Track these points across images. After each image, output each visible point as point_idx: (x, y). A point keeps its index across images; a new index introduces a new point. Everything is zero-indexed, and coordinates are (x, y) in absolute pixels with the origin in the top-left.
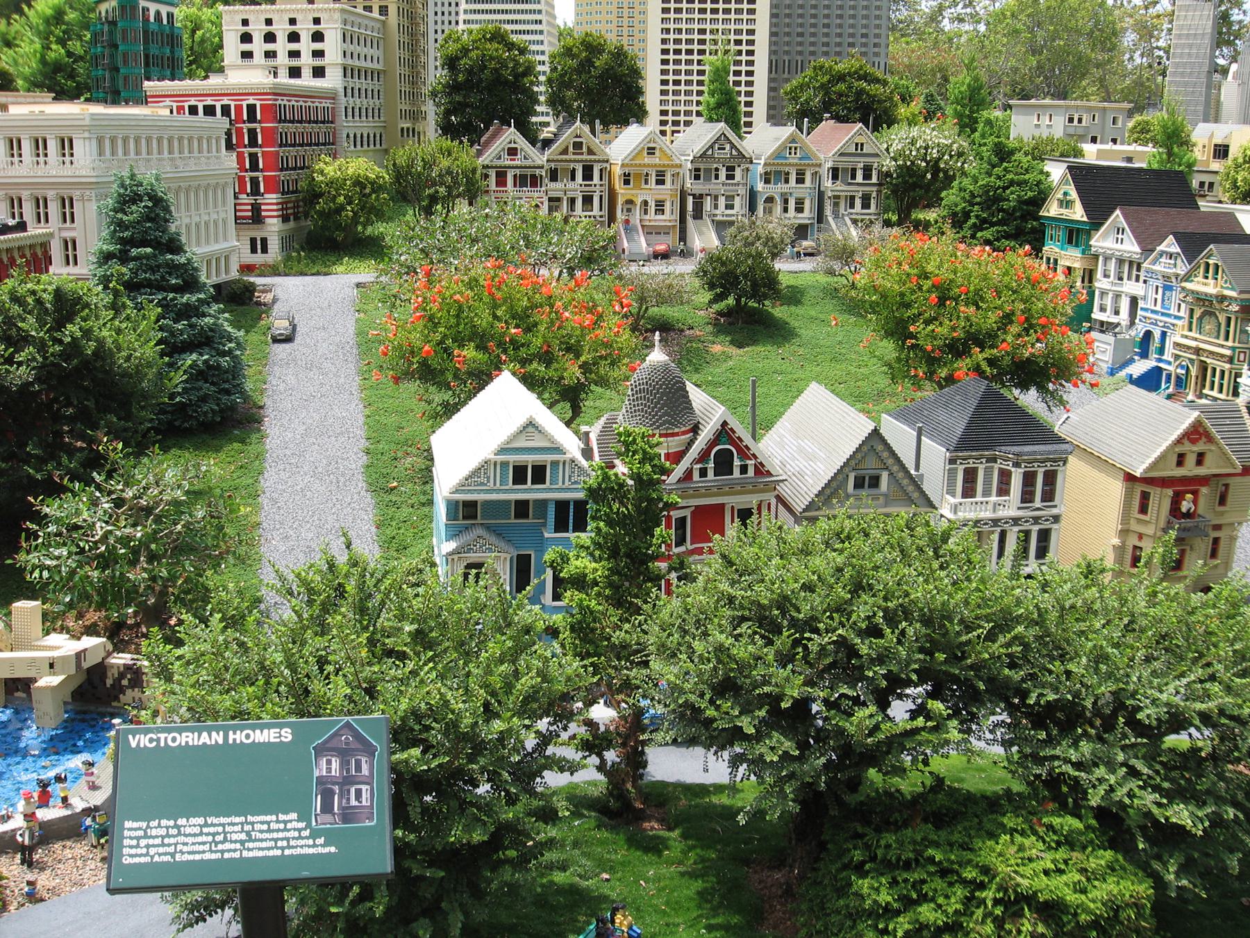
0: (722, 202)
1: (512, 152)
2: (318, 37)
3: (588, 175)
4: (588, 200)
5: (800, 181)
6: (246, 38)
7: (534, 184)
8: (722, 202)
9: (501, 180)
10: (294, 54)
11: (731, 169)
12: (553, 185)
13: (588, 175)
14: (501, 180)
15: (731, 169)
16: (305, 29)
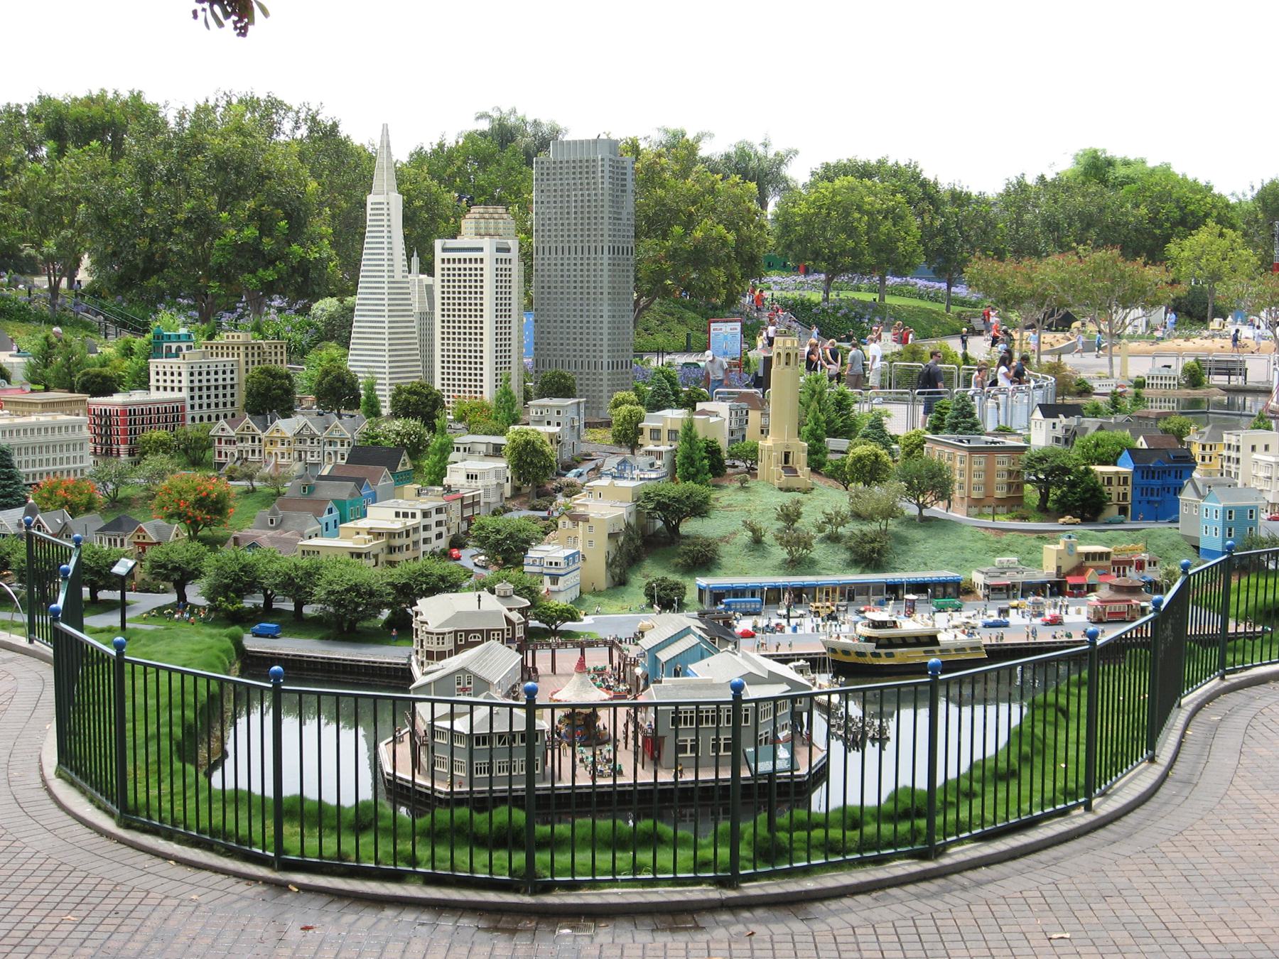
0: (309, 453)
1: (223, 430)
2: (180, 374)
3: (253, 441)
4: (253, 451)
5: (343, 445)
6: (158, 373)
7: (234, 443)
8: (309, 453)
9: (220, 442)
10: (172, 381)
11: (312, 439)
12: (242, 445)
13: (253, 441)
14: (220, 442)
15: (312, 439)
16: (175, 370)
